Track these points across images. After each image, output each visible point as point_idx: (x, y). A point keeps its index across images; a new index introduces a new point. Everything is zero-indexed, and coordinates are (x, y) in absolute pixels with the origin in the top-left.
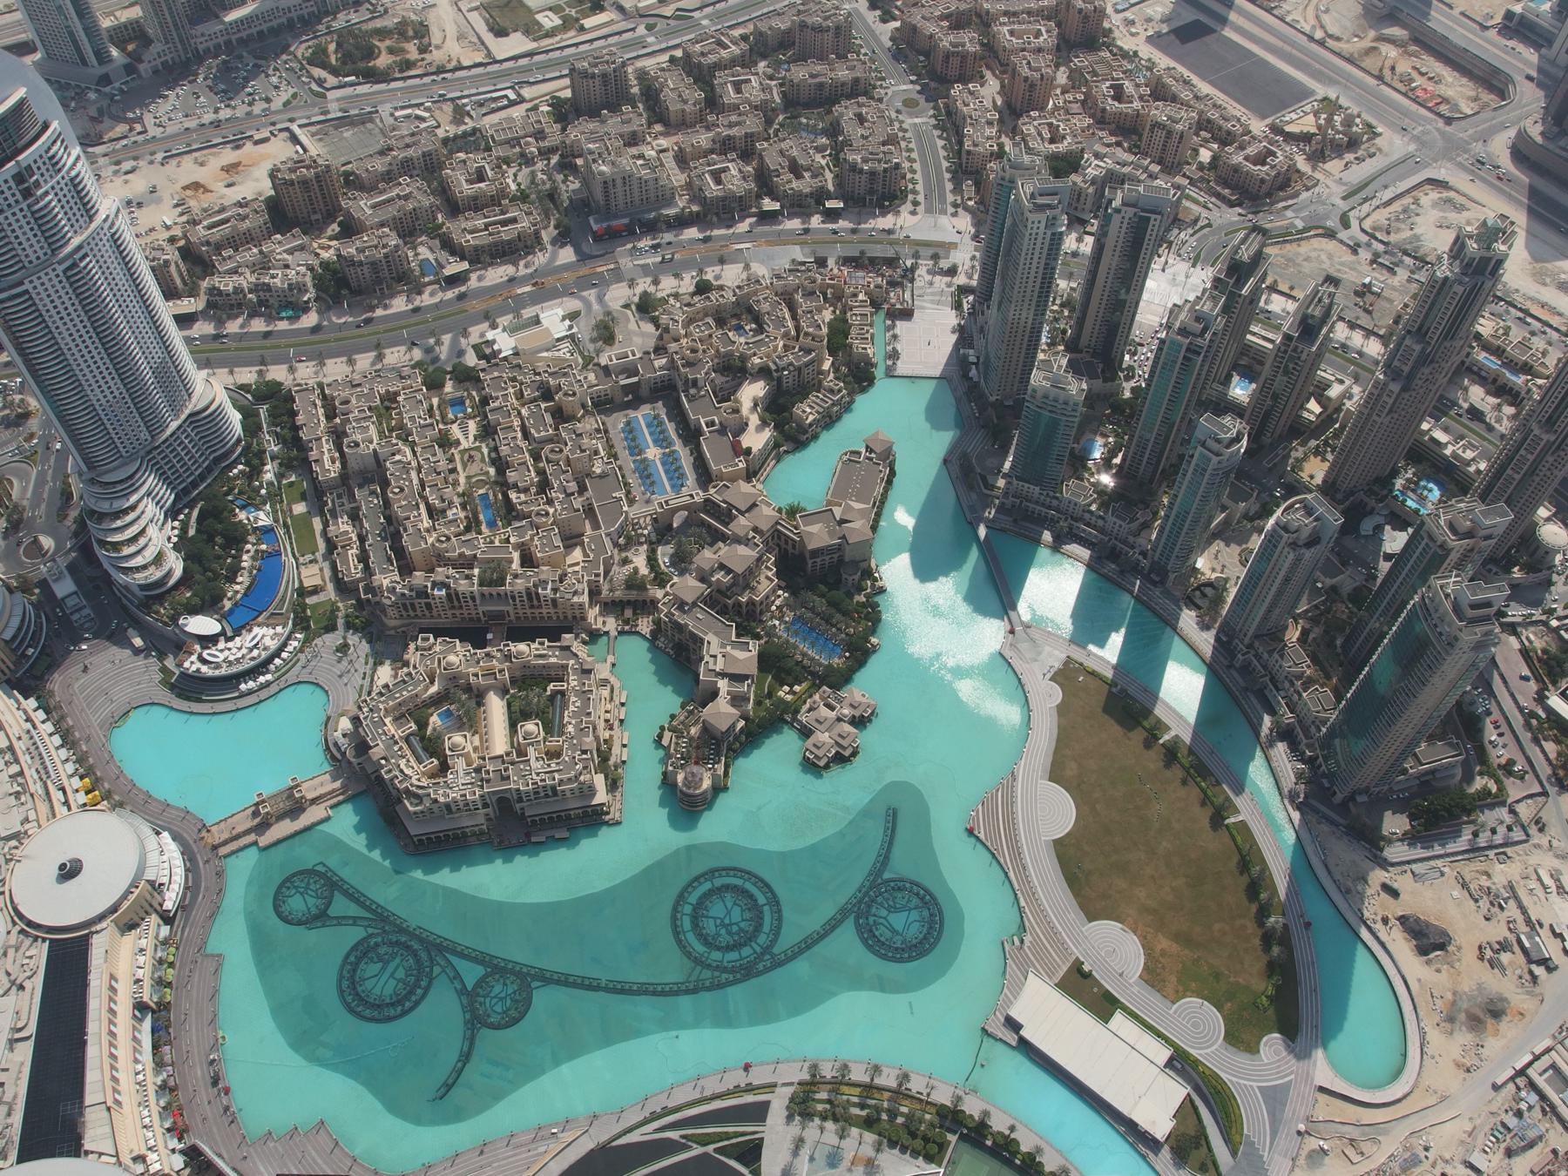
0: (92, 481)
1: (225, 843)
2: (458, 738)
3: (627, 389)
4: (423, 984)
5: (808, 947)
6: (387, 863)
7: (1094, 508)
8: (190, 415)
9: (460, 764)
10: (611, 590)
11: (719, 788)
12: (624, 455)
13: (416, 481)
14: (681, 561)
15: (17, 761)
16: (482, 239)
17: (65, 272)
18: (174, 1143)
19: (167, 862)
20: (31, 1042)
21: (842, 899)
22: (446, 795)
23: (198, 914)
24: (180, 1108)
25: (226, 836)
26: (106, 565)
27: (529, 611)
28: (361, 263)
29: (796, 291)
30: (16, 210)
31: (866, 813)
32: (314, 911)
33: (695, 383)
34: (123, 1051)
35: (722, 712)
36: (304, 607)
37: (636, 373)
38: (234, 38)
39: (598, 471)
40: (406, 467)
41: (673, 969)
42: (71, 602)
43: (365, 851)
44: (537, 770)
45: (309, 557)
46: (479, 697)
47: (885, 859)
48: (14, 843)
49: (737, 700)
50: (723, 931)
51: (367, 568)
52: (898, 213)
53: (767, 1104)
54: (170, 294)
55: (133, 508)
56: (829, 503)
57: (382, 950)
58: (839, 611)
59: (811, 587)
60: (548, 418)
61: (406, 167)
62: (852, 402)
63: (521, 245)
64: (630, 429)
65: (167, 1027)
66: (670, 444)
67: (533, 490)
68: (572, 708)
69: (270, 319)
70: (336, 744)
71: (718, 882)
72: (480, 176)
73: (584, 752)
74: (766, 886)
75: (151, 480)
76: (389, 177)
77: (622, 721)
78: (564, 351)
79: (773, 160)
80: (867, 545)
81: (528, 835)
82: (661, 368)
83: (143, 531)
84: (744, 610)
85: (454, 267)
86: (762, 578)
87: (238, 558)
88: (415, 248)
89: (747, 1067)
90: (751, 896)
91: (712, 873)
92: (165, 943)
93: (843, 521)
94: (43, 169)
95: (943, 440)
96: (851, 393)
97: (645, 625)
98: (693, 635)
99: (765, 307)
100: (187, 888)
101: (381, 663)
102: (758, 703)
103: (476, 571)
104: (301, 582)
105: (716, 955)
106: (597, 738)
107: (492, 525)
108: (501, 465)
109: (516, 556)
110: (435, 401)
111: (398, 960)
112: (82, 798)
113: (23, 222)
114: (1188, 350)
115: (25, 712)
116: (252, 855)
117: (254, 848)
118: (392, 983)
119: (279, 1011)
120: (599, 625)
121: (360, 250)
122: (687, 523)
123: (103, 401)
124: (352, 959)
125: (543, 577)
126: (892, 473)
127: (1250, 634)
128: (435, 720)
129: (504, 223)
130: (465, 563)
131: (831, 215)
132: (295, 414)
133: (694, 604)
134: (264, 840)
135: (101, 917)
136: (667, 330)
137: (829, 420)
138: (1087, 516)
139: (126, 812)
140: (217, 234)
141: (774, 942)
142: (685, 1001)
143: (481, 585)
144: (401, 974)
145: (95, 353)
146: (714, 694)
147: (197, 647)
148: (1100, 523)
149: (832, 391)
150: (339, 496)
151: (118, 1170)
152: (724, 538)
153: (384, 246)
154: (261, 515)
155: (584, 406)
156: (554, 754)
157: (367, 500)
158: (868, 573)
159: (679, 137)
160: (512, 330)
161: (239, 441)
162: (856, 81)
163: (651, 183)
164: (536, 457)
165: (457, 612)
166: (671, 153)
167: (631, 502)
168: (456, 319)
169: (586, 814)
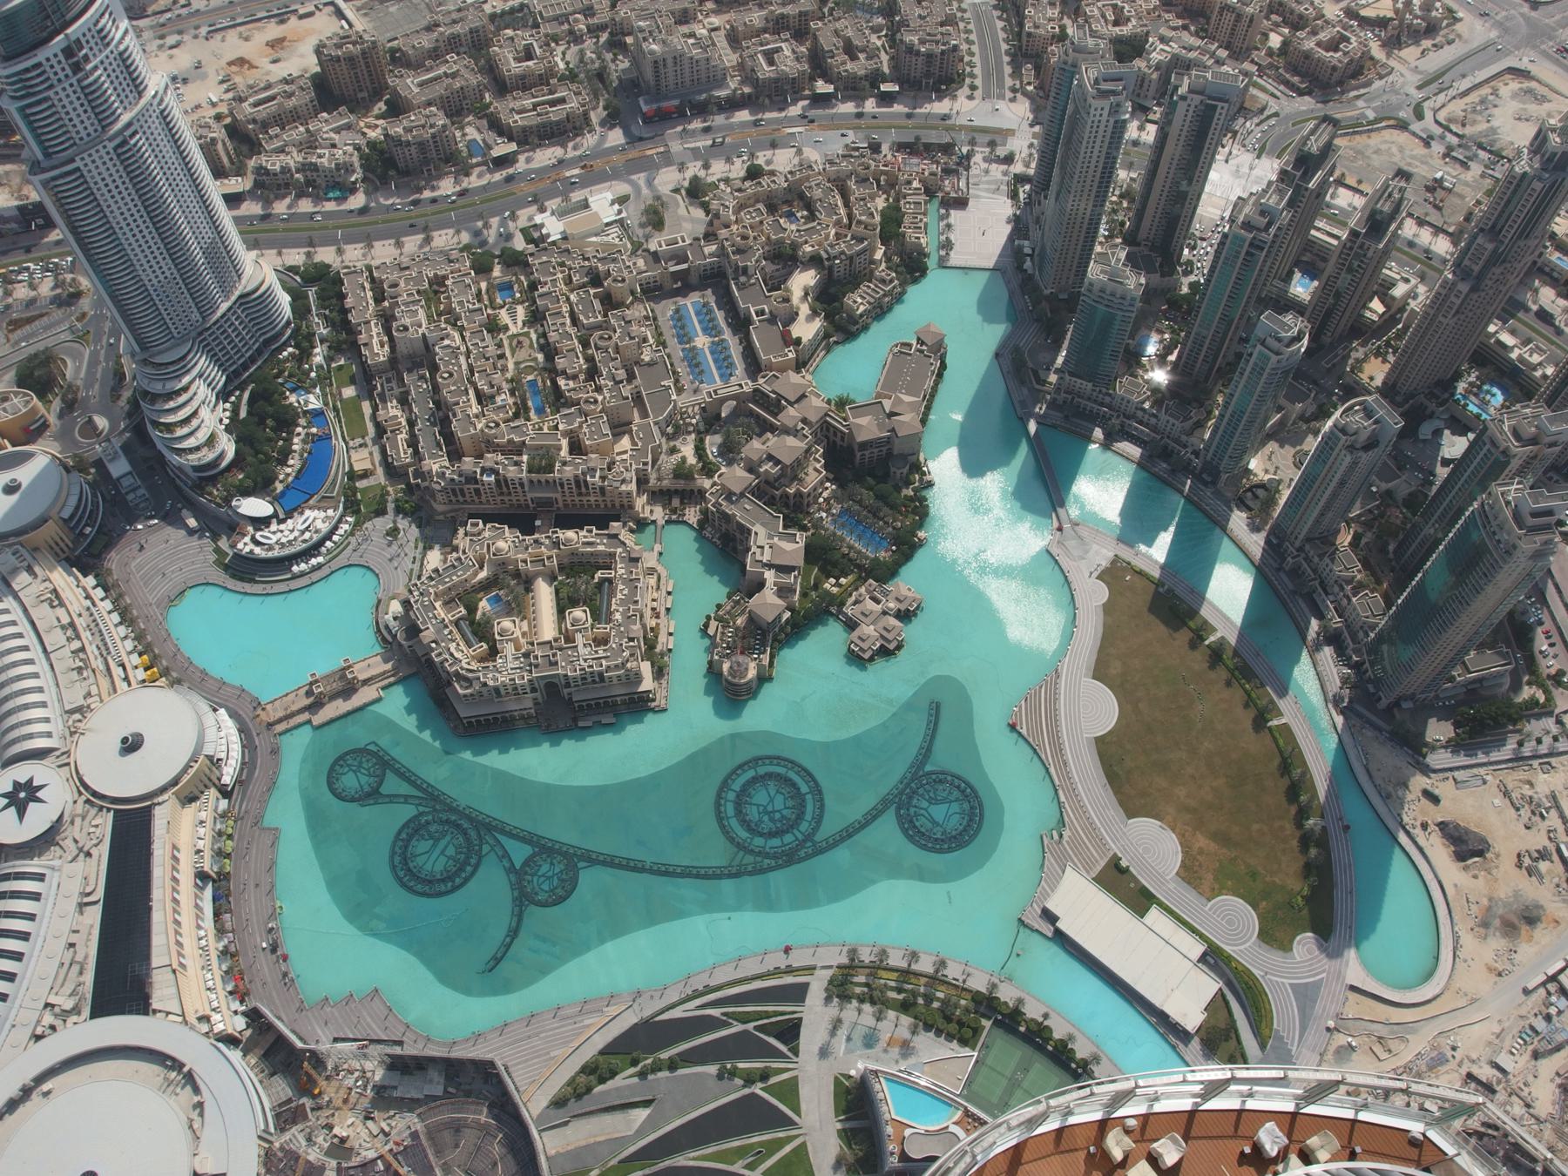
0: (145, 362)
1: (280, 721)
2: (506, 623)
3: (676, 276)
4: (473, 861)
5: (850, 836)
6: (437, 744)
7: (1147, 405)
8: (241, 297)
9: (509, 649)
10: (659, 479)
11: (764, 678)
12: (672, 342)
13: (464, 367)
14: (729, 451)
15: (78, 637)
16: (530, 119)
17: (115, 149)
18: (236, 1005)
19: (225, 738)
20: (99, 907)
21: (884, 789)
23: (256, 788)
24: (241, 972)
25: (281, 714)
26: (160, 446)
27: (577, 499)
28: (408, 143)
30: (66, 85)
31: (909, 706)
32: (367, 788)
33: (745, 271)
34: (187, 917)
35: (768, 603)
36: (354, 490)
37: (686, 260)
39: (647, 359)
40: (455, 352)
41: (716, 853)
42: (126, 482)
43: (416, 732)
44: (585, 656)
45: (359, 441)
46: (528, 583)
47: (926, 751)
48: (77, 716)
49: (783, 591)
50: (766, 818)
51: (416, 453)
52: (954, 98)
53: (806, 986)
55: (185, 389)
56: (879, 395)
57: (433, 828)
58: (887, 504)
59: (859, 479)
60: (597, 304)
61: (453, 44)
62: (903, 293)
63: (570, 126)
64: (679, 316)
65: (227, 896)
66: (720, 333)
67: (582, 377)
68: (619, 596)
69: (318, 199)
70: (387, 627)
71: (762, 770)
72: (528, 54)
73: (631, 639)
74: (808, 775)
75: (202, 362)
76: (436, 54)
77: (668, 610)
78: (613, 237)
79: (827, 41)
80: (916, 439)
81: (575, 720)
82: (712, 255)
83: (195, 413)
84: (792, 502)
85: (502, 148)
86: (810, 470)
87: (289, 441)
88: (462, 128)
89: (787, 950)
90: (794, 785)
91: (757, 761)
92: (224, 815)
93: (892, 414)
94: (92, 43)
95: (996, 333)
96: (903, 284)
97: (692, 515)
99: (818, 193)
100: (243, 763)
101: (431, 548)
102: (804, 595)
103: (525, 458)
104: (351, 465)
105: (759, 841)
106: (644, 626)
107: (540, 411)
108: (550, 351)
109: (564, 443)
110: (484, 285)
111: (448, 838)
112: (141, 674)
113: (73, 97)
114: (1251, 245)
115: (85, 589)
116: (305, 734)
117: (308, 727)
118: (443, 859)
119: (333, 883)
120: (647, 514)
121: (408, 130)
122: (735, 413)
123: (155, 281)
124: (404, 836)
125: (591, 465)
126: (943, 366)
127: (1301, 537)
128: (484, 605)
129: (553, 103)
130: (514, 449)
131: (886, 99)
132: (344, 297)
133: (742, 495)
134: (318, 719)
135: (163, 790)
136: (717, 216)
137: (880, 311)
138: (1139, 414)
139: (184, 688)
140: (263, 111)
141: (815, 830)
142: (727, 885)
143: (529, 471)
144: (451, 851)
145: (146, 232)
146: (760, 585)
147: (250, 529)
148: (1153, 421)
149: (883, 281)
150: (389, 380)
151: (186, 1029)
152: (772, 429)
153: (432, 126)
154: (312, 398)
155: (633, 293)
156: (601, 641)
157: (416, 385)
158: (917, 467)
159: (731, 16)
160: (560, 214)
163: (703, 63)
164: (585, 344)
165: (506, 499)
166: (723, 32)
167: (680, 391)
168: (505, 199)
169: (632, 701)
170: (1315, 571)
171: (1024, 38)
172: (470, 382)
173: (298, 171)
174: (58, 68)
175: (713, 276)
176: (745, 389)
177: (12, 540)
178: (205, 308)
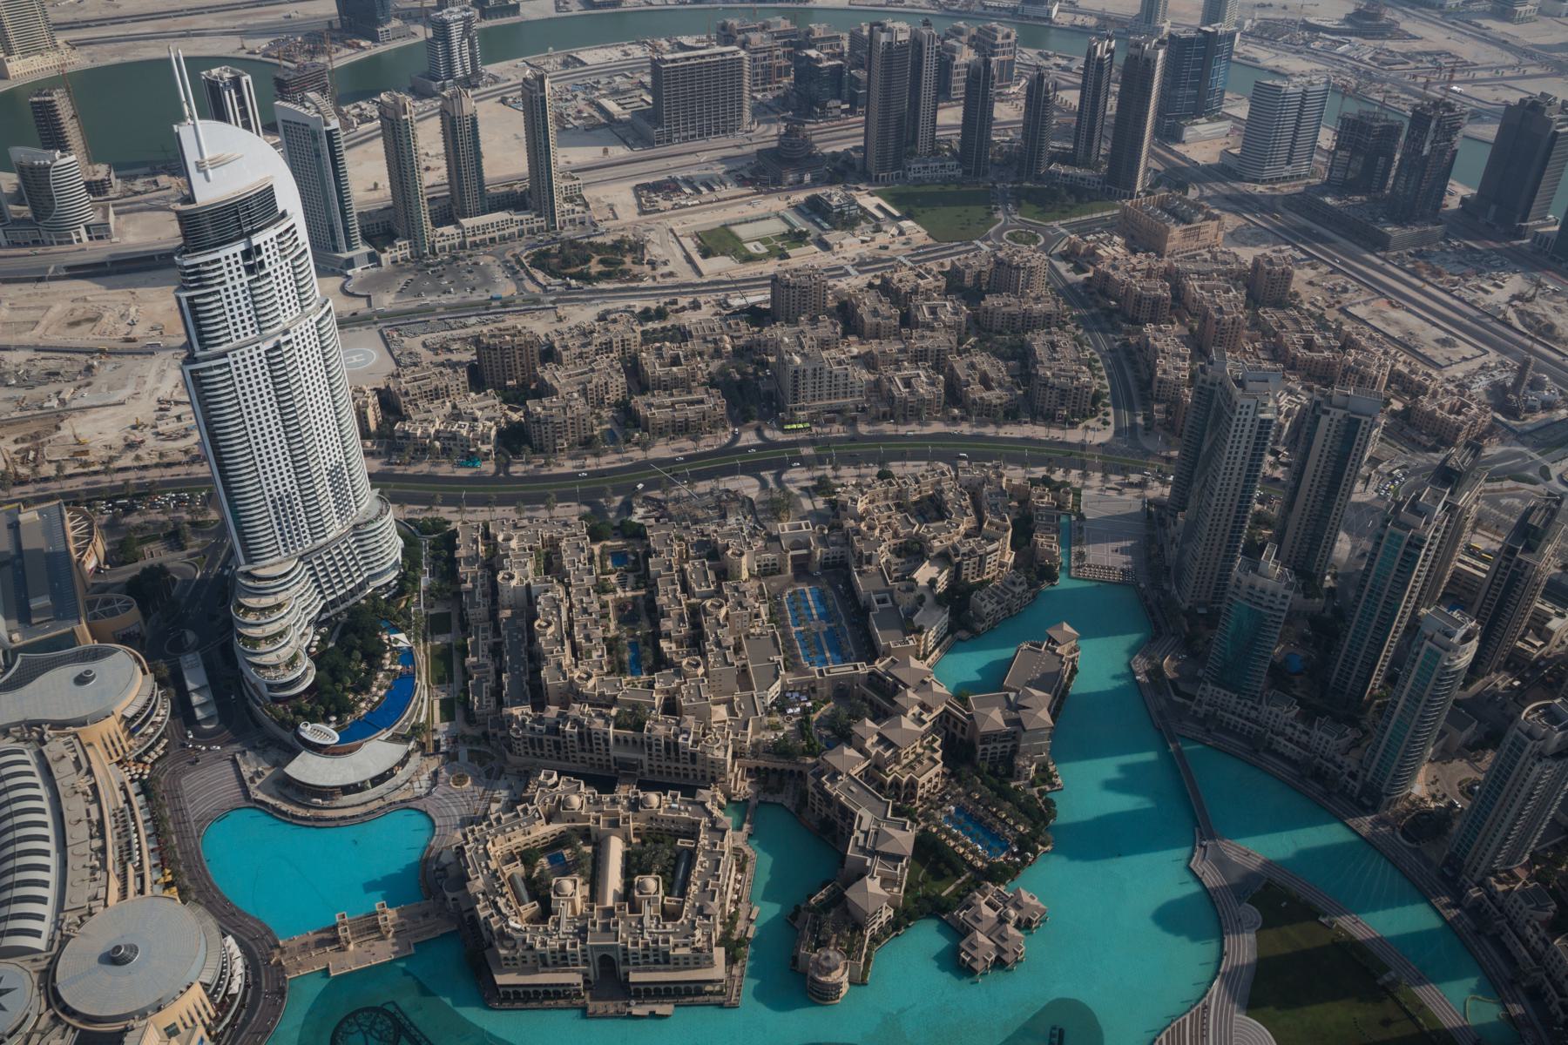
2: (567, 884)
9: (565, 912)
13: (564, 618)
15: (103, 836)
22: (544, 943)
27: (664, 764)
29: (982, 484)
37: (807, 545)
38: (468, 240)
49: (886, 882)
54: (365, 434)
60: (711, 576)
68: (698, 868)
73: (707, 917)
83: (281, 634)
94: (271, 252)
103: (614, 712)
109: (658, 700)
112: (158, 890)
114: (1409, 544)
115: (126, 793)
123: (274, 492)
127: (1481, 868)
130: (602, 703)
132: (456, 547)
136: (844, 507)
146: (862, 873)
154: (402, 636)
156: (670, 914)
162: (1048, 316)
163: (841, 381)
165: (587, 755)
170: (1500, 909)
171: (1155, 385)
173: (437, 438)
174: (234, 267)
175: (834, 565)
176: (860, 670)
177: (72, 729)
178: (316, 529)
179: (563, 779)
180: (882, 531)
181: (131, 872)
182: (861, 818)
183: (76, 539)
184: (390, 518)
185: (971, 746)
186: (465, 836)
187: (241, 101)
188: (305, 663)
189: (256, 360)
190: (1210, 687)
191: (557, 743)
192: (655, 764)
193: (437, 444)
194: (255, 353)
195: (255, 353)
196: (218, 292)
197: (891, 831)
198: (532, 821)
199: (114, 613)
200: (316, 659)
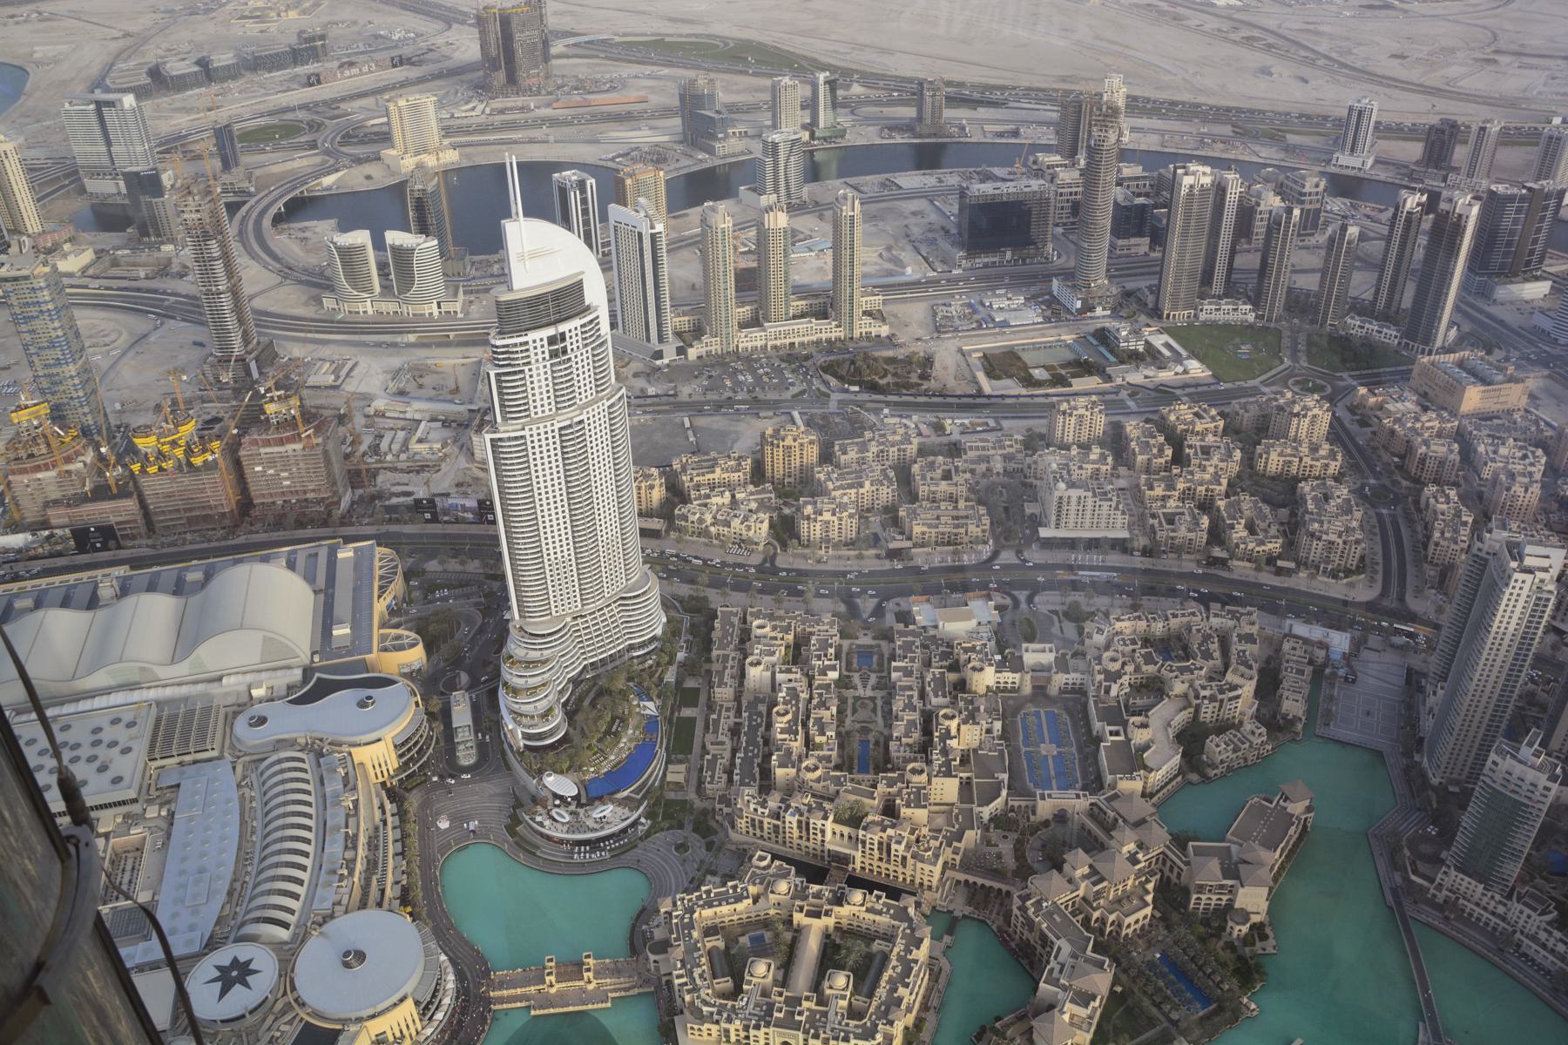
15: (355, 848)
17: (561, 429)
27: (875, 863)
51: (730, 780)
68: (890, 971)
98: (1044, 939)
115: (384, 812)
150: (728, 710)
154: (650, 704)
161: (654, 638)
171: (1431, 547)
172: (805, 725)
174: (539, 350)
175: (1073, 691)
179: (777, 863)
180: (1124, 664)
181: (374, 882)
182: (1059, 949)
183: (381, 578)
184: (655, 594)
185: (1186, 892)
186: (675, 904)
187: (584, 201)
188: (558, 717)
189: (550, 435)
190: (1453, 873)
191: (776, 827)
192: (867, 861)
193: (712, 529)
194: (549, 429)
195: (549, 429)
196: (522, 372)
197: (1089, 967)
198: (739, 899)
199: (401, 648)
200: (570, 715)
